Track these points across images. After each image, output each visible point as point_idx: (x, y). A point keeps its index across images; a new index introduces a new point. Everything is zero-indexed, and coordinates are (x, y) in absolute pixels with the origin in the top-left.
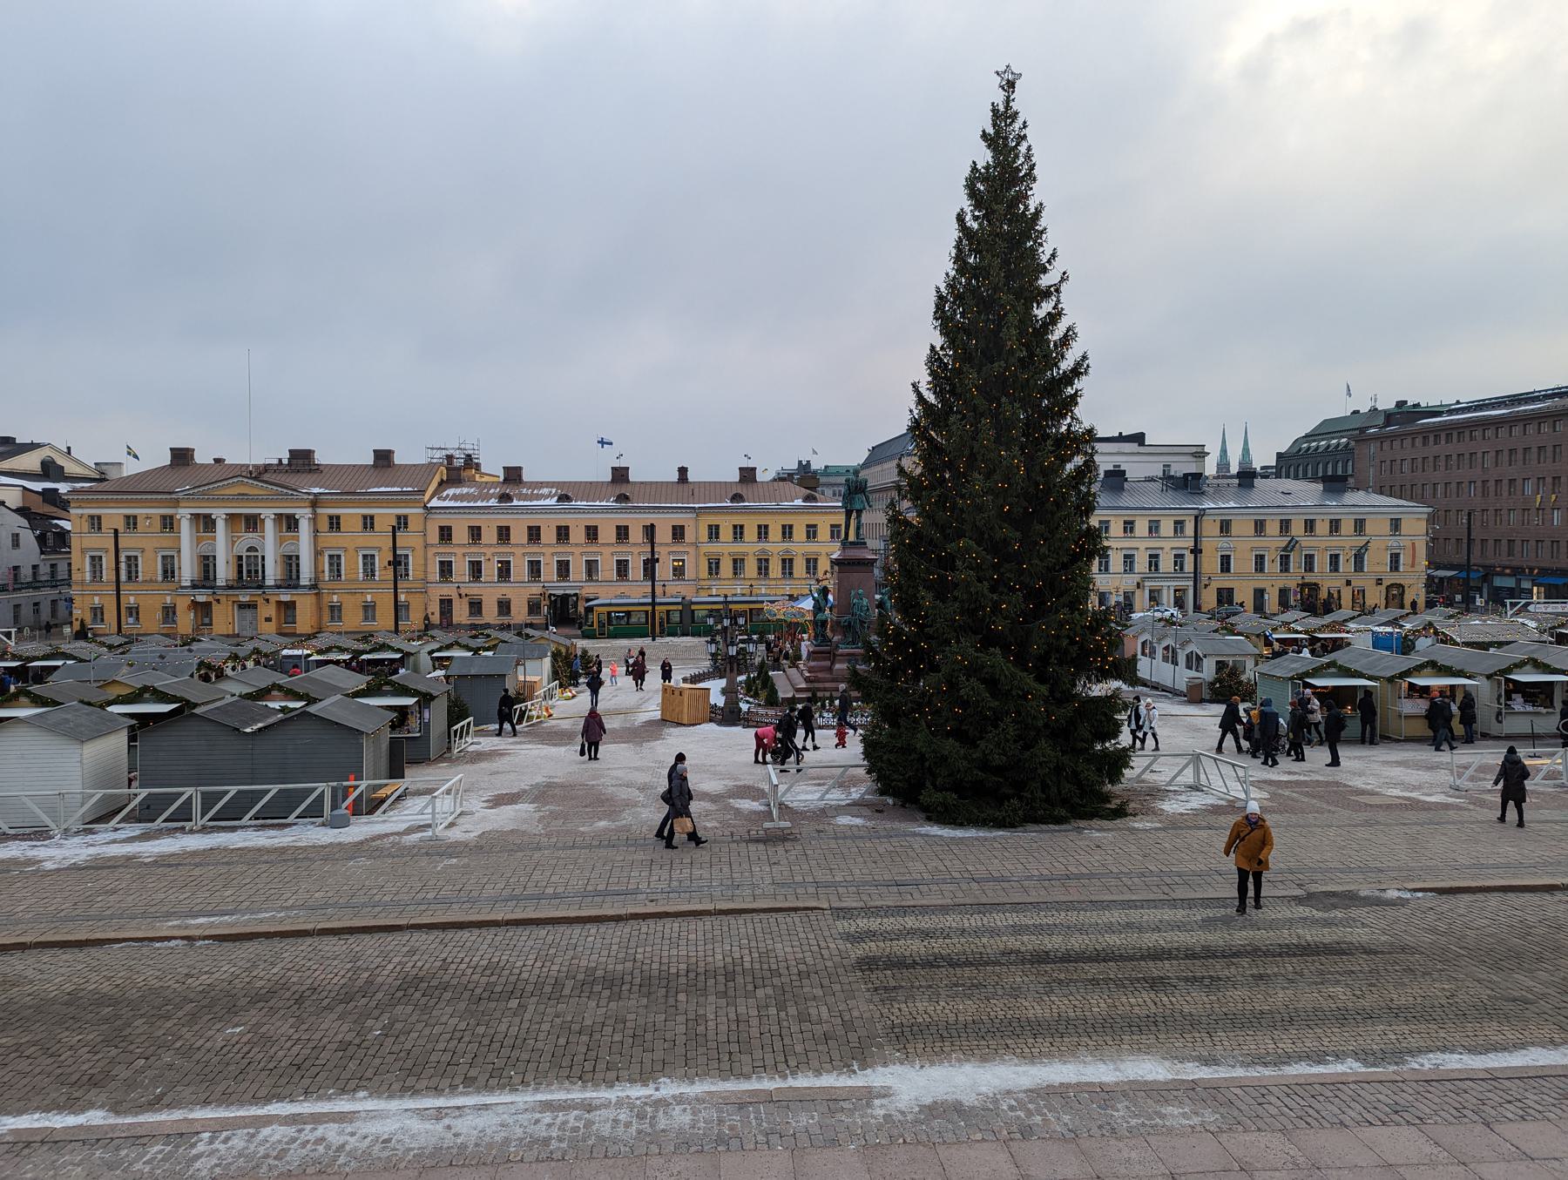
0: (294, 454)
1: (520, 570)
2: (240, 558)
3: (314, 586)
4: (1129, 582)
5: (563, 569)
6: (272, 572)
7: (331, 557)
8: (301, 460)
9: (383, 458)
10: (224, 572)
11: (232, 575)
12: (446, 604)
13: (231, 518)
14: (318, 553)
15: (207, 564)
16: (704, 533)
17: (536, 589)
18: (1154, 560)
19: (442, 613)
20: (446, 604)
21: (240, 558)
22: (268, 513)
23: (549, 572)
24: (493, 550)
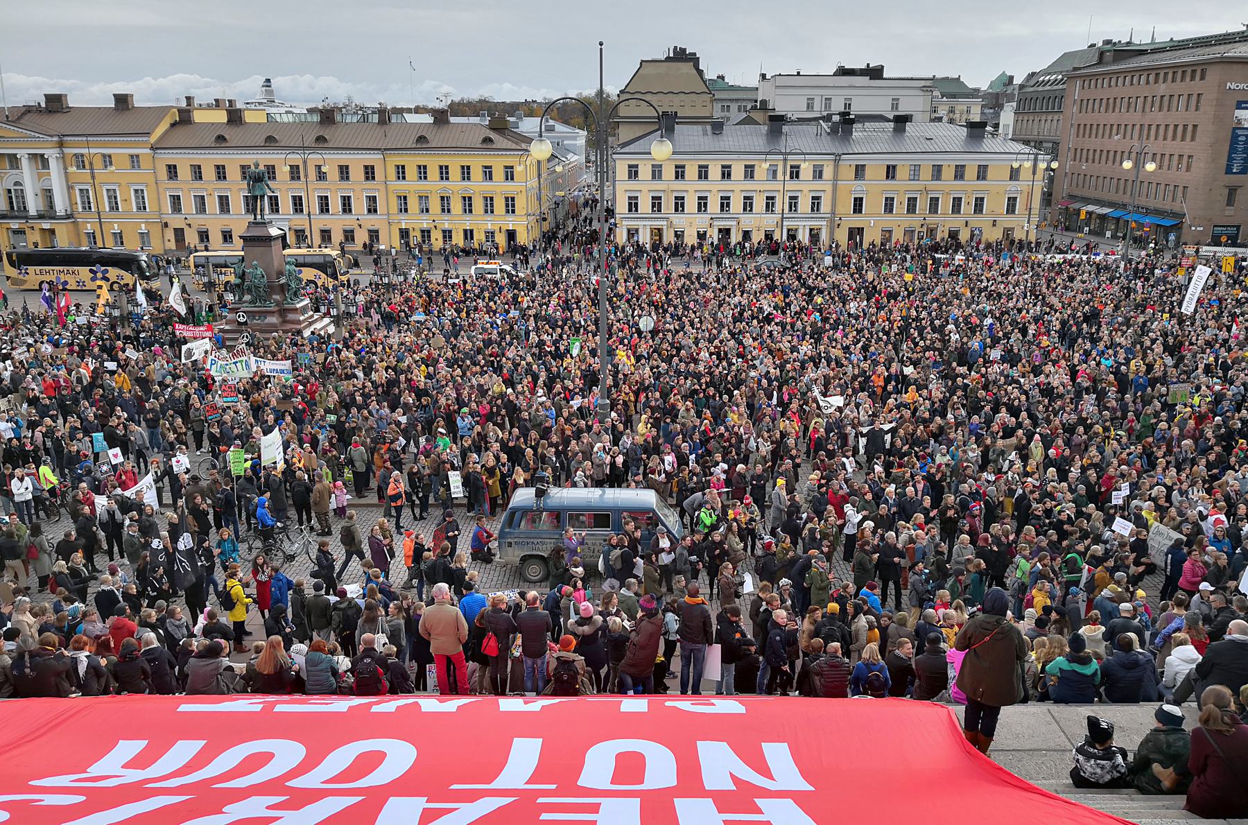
0: (49, 98)
2: (9, 191)
3: (68, 217)
6: (33, 207)
7: (81, 190)
8: (55, 103)
9: (122, 101)
12: (179, 233)
14: (70, 188)
16: (392, 173)
19: (177, 241)
20: (179, 233)
21: (9, 191)
22: (22, 153)
24: (213, 186)
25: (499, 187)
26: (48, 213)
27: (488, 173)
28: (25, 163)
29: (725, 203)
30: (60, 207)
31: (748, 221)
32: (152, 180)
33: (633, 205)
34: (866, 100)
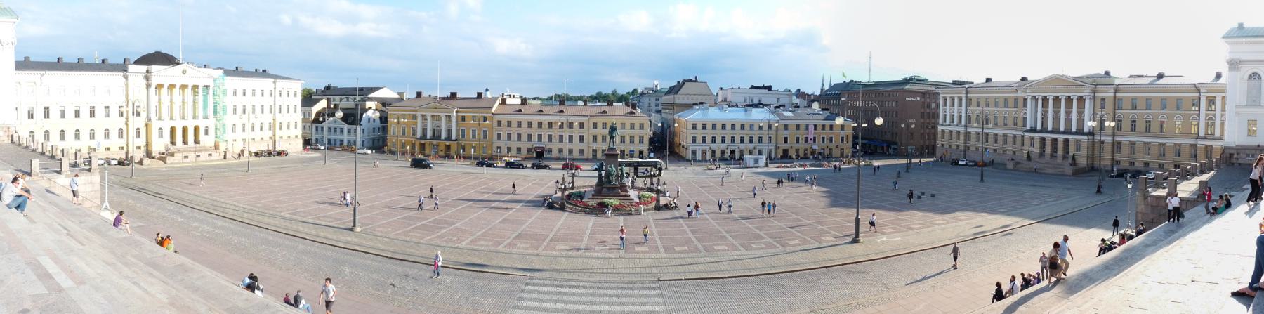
1: (525, 137)
5: (540, 137)
6: (443, 136)
10: (429, 134)
15: (424, 130)
17: (529, 145)
18: (760, 139)
22: (443, 115)
23: (535, 138)
25: (637, 132)
26: (449, 138)
27: (632, 127)
29: (733, 139)
31: (742, 146)
33: (694, 140)
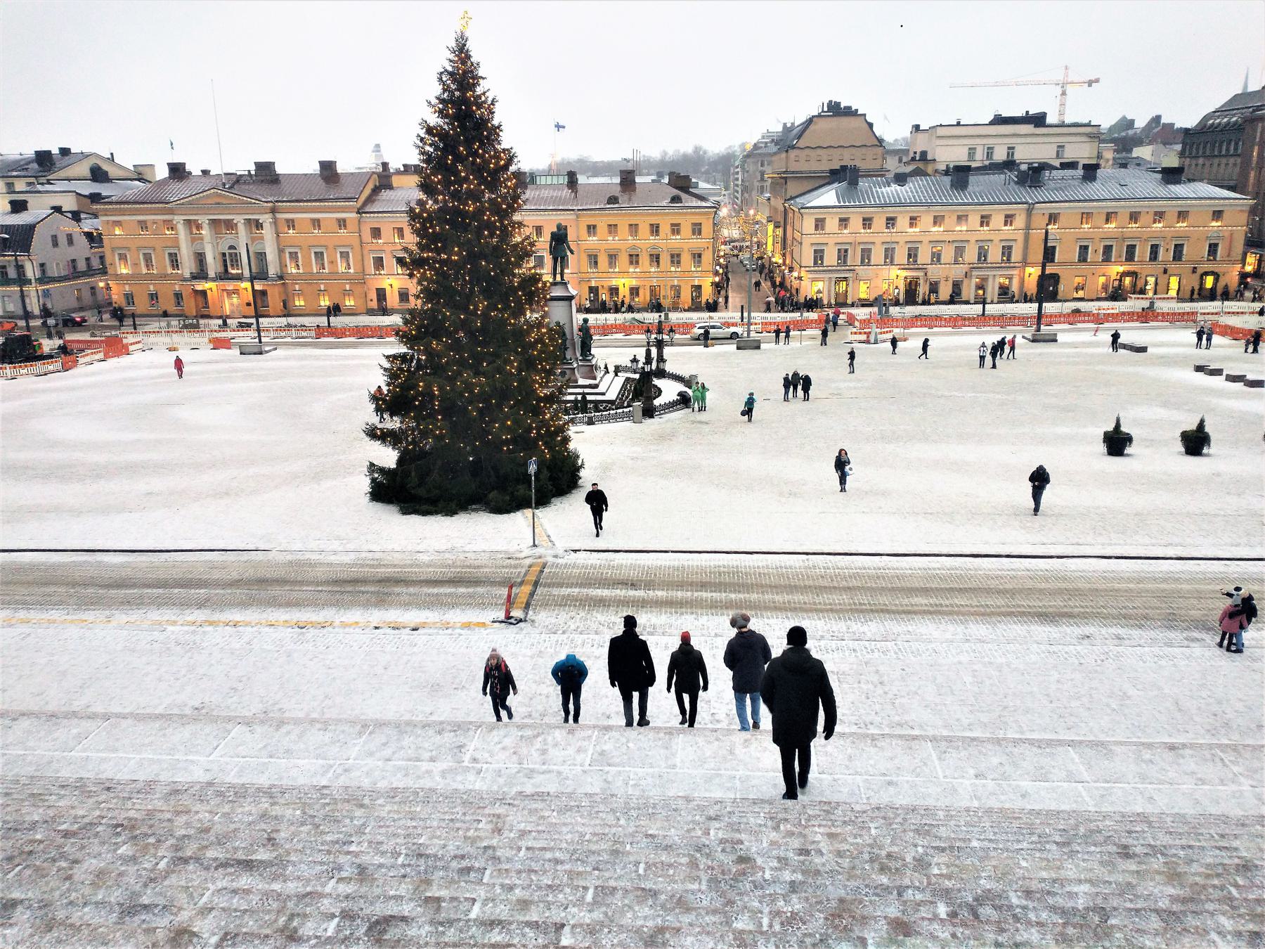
2: (224, 254)
3: (281, 278)
4: (957, 272)
8: (266, 173)
9: (328, 170)
11: (220, 269)
13: (214, 223)
14: (281, 251)
15: (200, 258)
16: (584, 230)
22: (239, 219)
28: (241, 227)
30: (272, 271)
32: (356, 243)
34: (1031, 150)
